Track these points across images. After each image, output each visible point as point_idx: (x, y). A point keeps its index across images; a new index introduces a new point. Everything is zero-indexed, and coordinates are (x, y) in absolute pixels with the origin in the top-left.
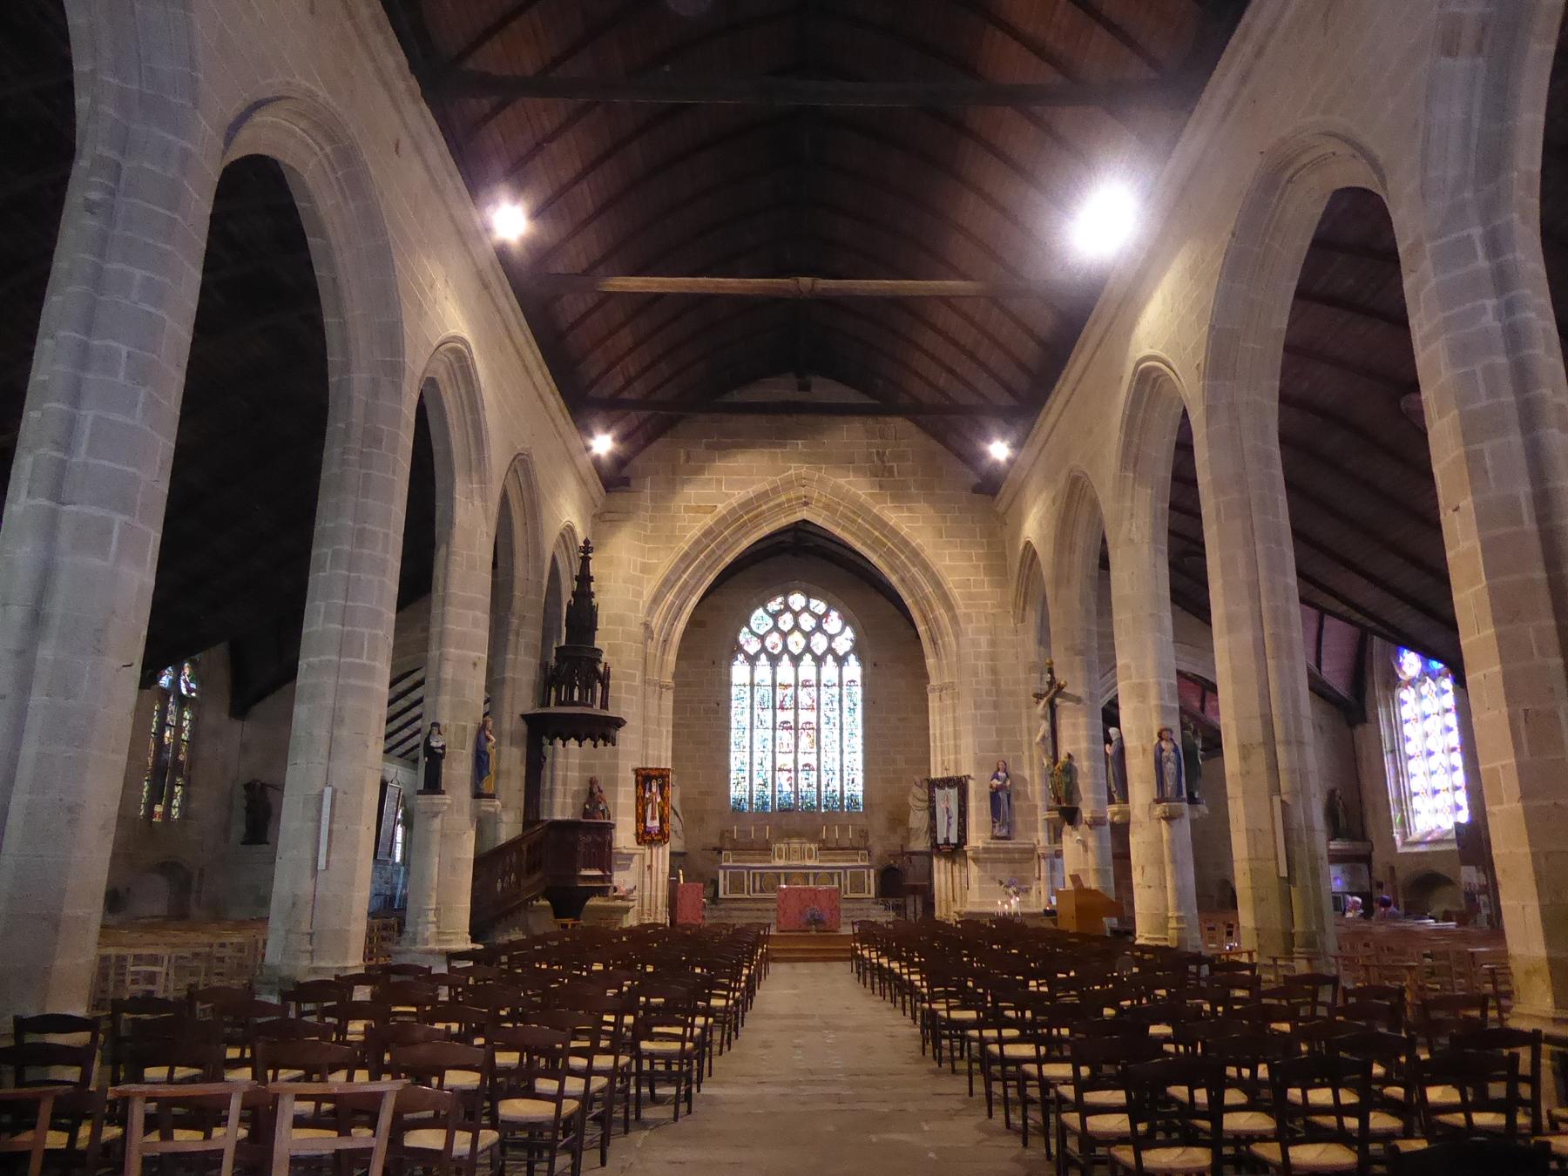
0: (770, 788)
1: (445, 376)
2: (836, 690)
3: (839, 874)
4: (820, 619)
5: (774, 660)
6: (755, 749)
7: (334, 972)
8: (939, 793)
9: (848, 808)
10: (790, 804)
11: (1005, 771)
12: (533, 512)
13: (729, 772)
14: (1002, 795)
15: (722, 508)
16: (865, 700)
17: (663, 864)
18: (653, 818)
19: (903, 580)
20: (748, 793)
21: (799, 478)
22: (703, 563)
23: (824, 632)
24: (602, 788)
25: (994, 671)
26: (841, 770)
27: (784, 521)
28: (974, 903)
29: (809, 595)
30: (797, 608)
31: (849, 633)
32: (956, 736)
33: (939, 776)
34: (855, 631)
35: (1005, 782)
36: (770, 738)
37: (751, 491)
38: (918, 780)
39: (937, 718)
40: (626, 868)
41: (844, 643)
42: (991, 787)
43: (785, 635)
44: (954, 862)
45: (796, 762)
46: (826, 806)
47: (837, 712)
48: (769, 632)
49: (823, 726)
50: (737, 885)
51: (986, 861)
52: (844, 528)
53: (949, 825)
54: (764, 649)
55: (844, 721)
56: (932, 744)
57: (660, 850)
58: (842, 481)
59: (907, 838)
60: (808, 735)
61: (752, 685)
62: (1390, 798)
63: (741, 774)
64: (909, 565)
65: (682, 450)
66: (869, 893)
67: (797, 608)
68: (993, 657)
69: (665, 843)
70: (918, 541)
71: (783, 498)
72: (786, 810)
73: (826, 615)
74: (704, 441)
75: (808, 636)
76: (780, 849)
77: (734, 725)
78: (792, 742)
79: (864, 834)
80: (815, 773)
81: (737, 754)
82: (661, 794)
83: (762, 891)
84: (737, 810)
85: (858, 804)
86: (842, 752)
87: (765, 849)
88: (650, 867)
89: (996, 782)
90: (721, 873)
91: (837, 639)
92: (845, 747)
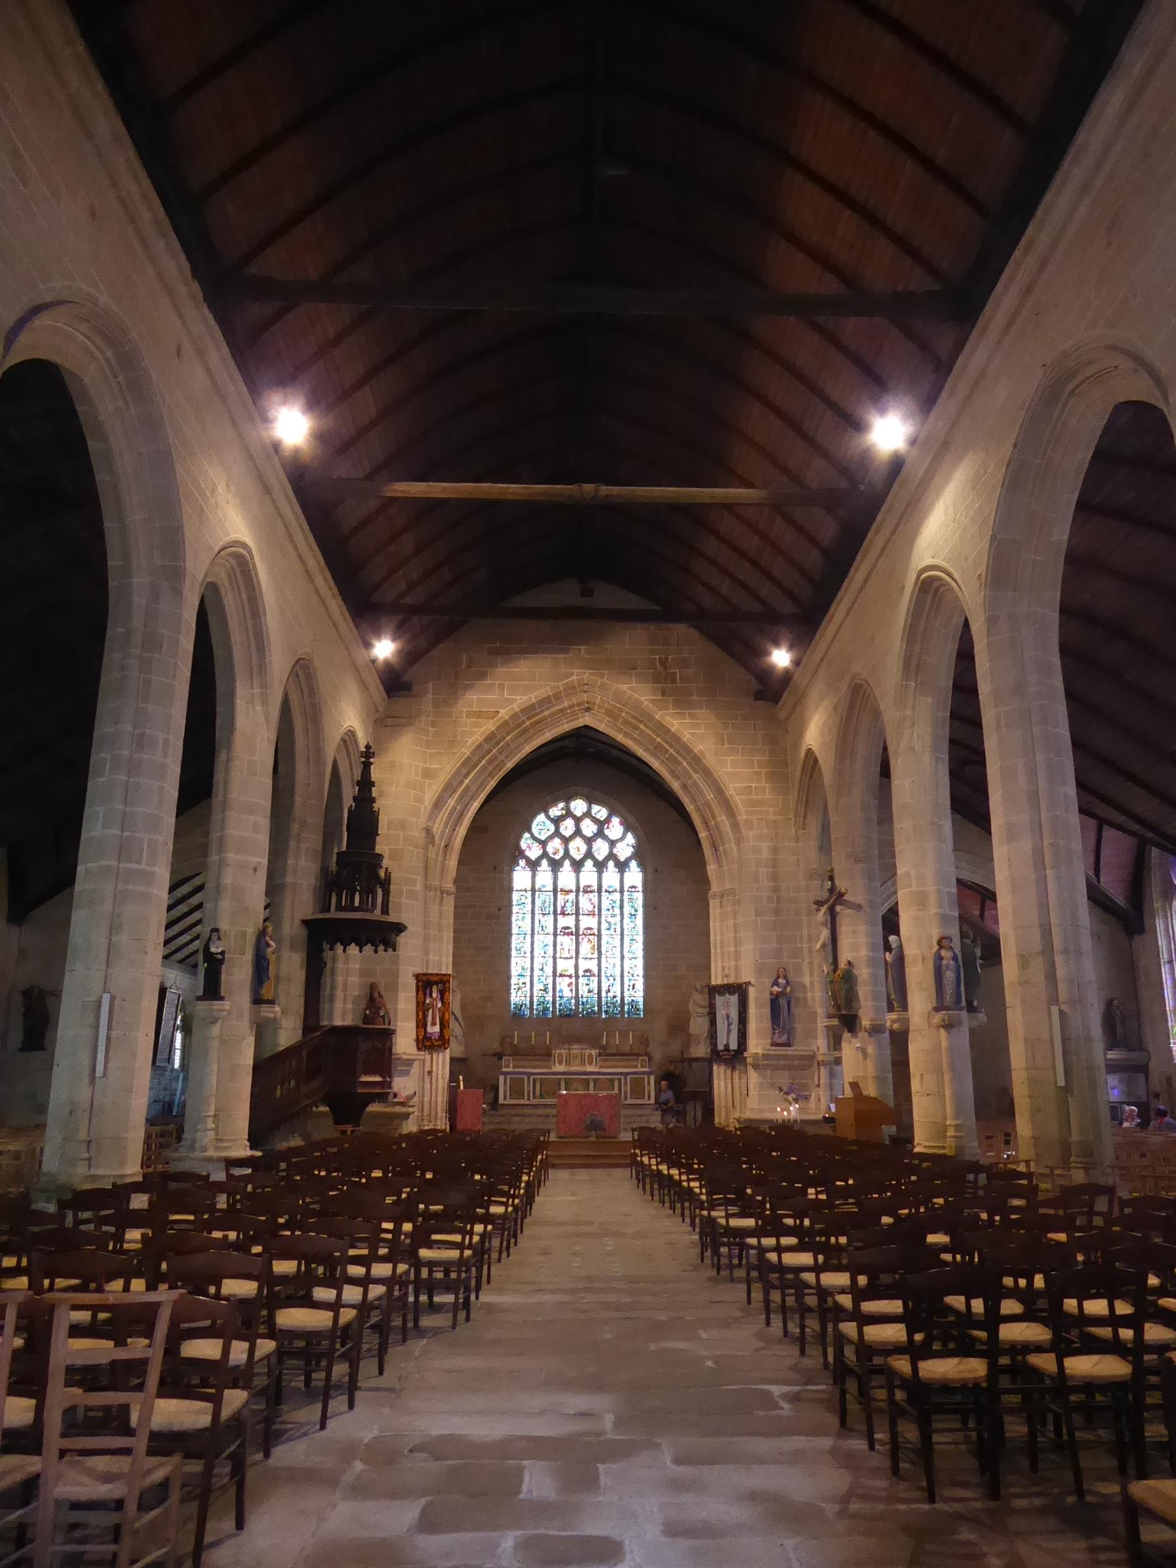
0: (551, 994)
1: (226, 582)
2: (617, 896)
3: (620, 1080)
4: (601, 824)
5: (555, 865)
6: (536, 953)
7: (112, 1180)
8: (719, 1000)
9: (628, 1013)
10: (571, 1010)
11: (785, 978)
12: (315, 715)
13: (509, 977)
14: (783, 1002)
15: (504, 714)
16: (645, 906)
17: (443, 1067)
18: (434, 1024)
19: (684, 786)
20: (528, 999)
21: (582, 683)
22: (484, 768)
23: (605, 838)
24: (383, 993)
25: (774, 877)
26: (622, 976)
27: (566, 727)
28: (752, 1110)
29: (590, 801)
30: (578, 813)
31: (630, 839)
32: (737, 943)
33: (719, 982)
34: (636, 836)
35: (785, 988)
36: (551, 944)
37: (533, 697)
38: (698, 986)
39: (718, 924)
40: (406, 1073)
41: (625, 850)
42: (771, 994)
43: (566, 841)
44: (733, 1069)
45: (576, 967)
46: (606, 1012)
47: (618, 917)
48: (551, 838)
49: (604, 932)
50: (516, 1089)
51: (766, 1067)
52: (626, 735)
53: (729, 1031)
54: (545, 855)
55: (625, 927)
56: (712, 951)
57: (441, 1056)
58: (625, 687)
59: (687, 1045)
60: (589, 940)
61: (533, 890)
62: (1168, 1008)
63: (522, 980)
64: (691, 771)
65: (465, 656)
66: (649, 1099)
67: (578, 813)
68: (774, 864)
69: (446, 1049)
70: (701, 747)
71: (566, 704)
72: (568, 1016)
73: (608, 820)
74: (487, 646)
75: (589, 841)
76: (560, 1055)
77: (515, 930)
78: (573, 947)
79: (644, 1041)
80: (596, 979)
81: (518, 960)
82: (442, 999)
83: (542, 1096)
84: (518, 1015)
85: (638, 1010)
86: (622, 958)
87: (547, 1055)
88: (430, 1073)
89: (776, 989)
90: (501, 1078)
91: (619, 845)
92: (625, 953)
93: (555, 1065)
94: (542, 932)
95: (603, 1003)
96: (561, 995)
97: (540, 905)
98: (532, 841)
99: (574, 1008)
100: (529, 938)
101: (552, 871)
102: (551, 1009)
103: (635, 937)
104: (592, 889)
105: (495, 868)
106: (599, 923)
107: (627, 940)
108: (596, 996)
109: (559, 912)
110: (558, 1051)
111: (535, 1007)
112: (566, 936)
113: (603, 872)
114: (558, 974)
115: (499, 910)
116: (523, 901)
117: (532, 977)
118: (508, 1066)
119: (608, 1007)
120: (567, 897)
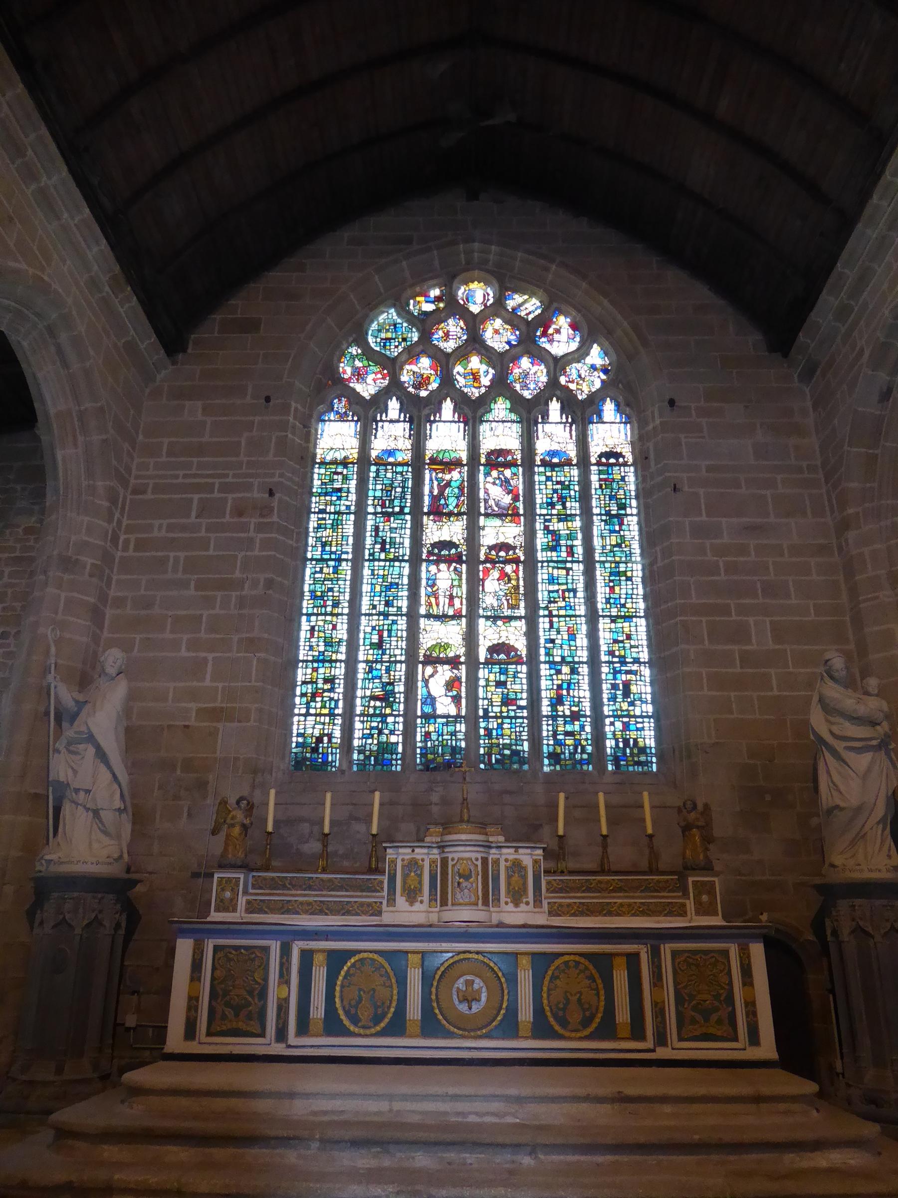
3: (633, 959)
6: (365, 608)
9: (616, 760)
10: (454, 750)
13: (294, 663)
26: (594, 662)
31: (596, 356)
34: (613, 347)
45: (471, 638)
46: (555, 757)
54: (395, 388)
55: (597, 542)
60: (504, 576)
61: (364, 460)
66: (754, 1038)
73: (544, 322)
76: (413, 865)
83: (333, 1026)
85: (643, 750)
86: (593, 617)
90: (184, 948)
91: (573, 370)
93: (392, 901)
94: (383, 556)
95: (545, 734)
96: (428, 709)
97: (378, 494)
98: (366, 363)
99: (463, 744)
100: (346, 567)
101: (411, 421)
102: (400, 749)
103: (622, 567)
104: (509, 458)
105: (268, 399)
106: (530, 534)
107: (601, 575)
108: (525, 713)
109: (426, 510)
110: (405, 853)
111: (356, 743)
112: (443, 566)
113: (536, 423)
114: (421, 659)
115: (271, 493)
116: (337, 485)
117: (351, 663)
118: (228, 906)
119: (558, 743)
120: (447, 477)
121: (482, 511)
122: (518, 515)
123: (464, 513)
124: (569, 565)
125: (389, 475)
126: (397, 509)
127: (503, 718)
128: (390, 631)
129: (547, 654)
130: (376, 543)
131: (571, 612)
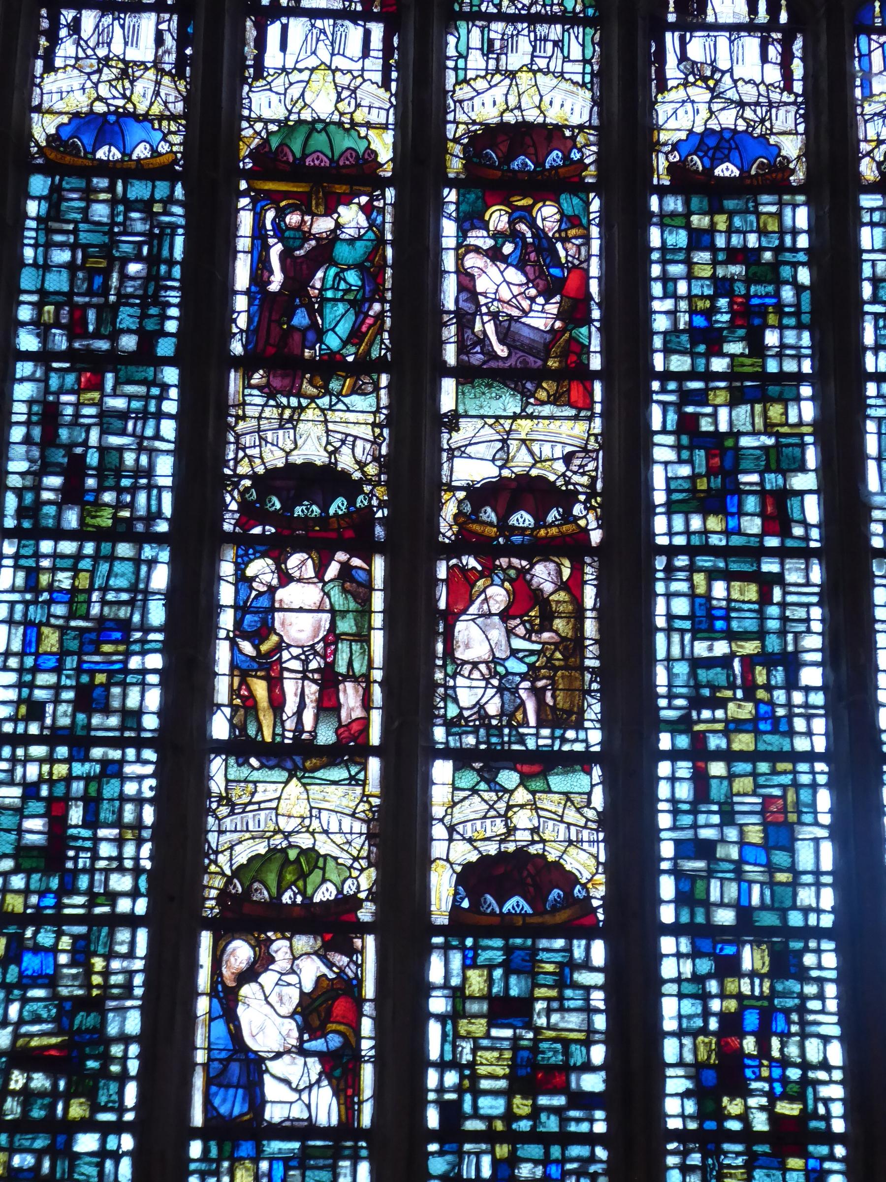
97: (57, 282)
120: (323, 225)
121: (450, 355)
122: (587, 376)
123: (380, 366)
124: (770, 566)
125: (100, 212)
126: (129, 342)
127: (514, 1138)
128: (92, 804)
129: (682, 899)
130: (45, 468)
131: (774, 742)
